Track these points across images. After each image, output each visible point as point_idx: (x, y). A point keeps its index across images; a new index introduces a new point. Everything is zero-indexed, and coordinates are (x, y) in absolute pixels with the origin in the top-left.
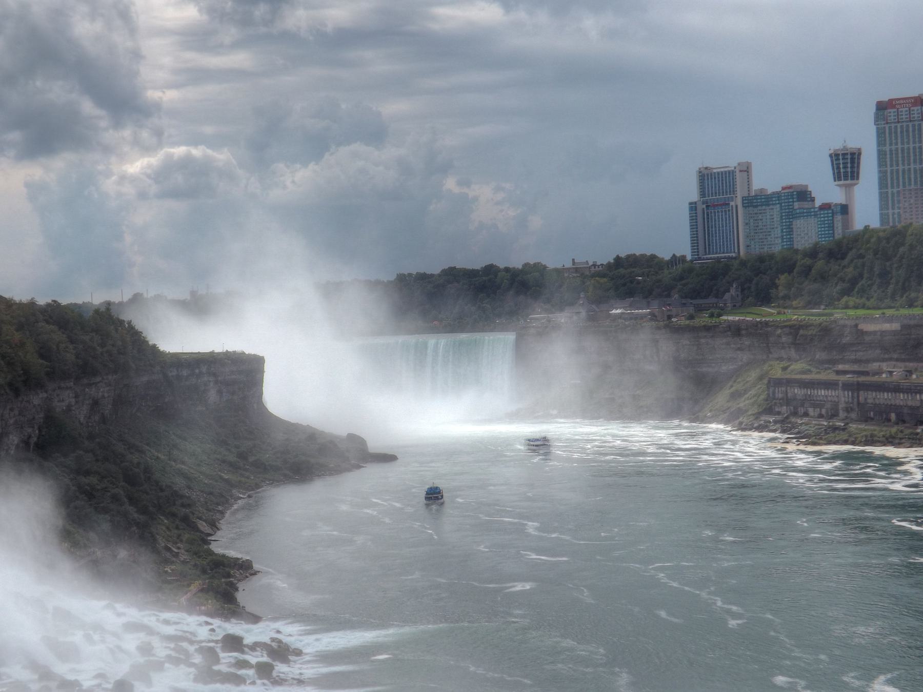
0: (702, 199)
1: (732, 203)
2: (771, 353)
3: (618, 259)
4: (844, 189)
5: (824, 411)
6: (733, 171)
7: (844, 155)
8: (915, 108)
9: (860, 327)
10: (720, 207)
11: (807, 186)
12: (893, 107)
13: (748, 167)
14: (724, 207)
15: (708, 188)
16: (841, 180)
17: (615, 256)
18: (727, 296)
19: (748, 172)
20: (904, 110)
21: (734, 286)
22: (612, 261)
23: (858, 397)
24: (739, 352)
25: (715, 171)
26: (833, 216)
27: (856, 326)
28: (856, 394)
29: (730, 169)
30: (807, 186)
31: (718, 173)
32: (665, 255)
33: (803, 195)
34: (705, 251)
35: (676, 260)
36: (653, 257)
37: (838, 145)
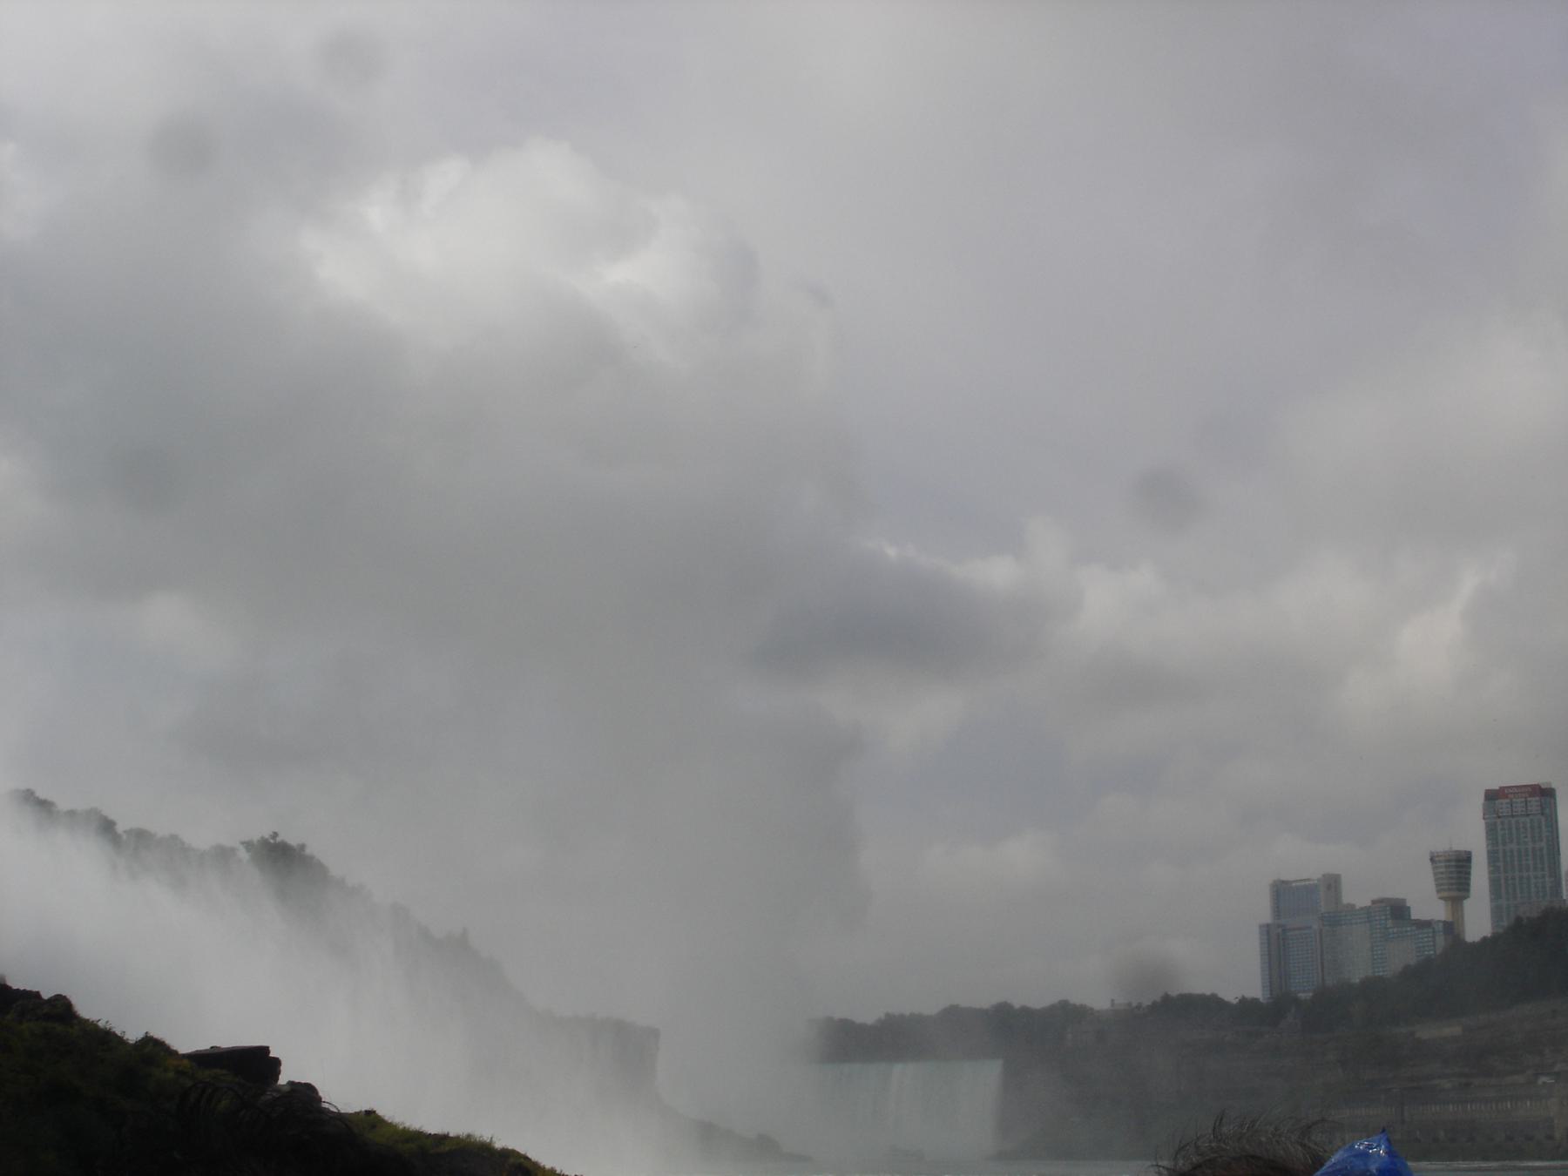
8: (1534, 799)
12: (1506, 796)
25: (1294, 884)
26: (1434, 937)
29: (1311, 882)
33: (1398, 910)
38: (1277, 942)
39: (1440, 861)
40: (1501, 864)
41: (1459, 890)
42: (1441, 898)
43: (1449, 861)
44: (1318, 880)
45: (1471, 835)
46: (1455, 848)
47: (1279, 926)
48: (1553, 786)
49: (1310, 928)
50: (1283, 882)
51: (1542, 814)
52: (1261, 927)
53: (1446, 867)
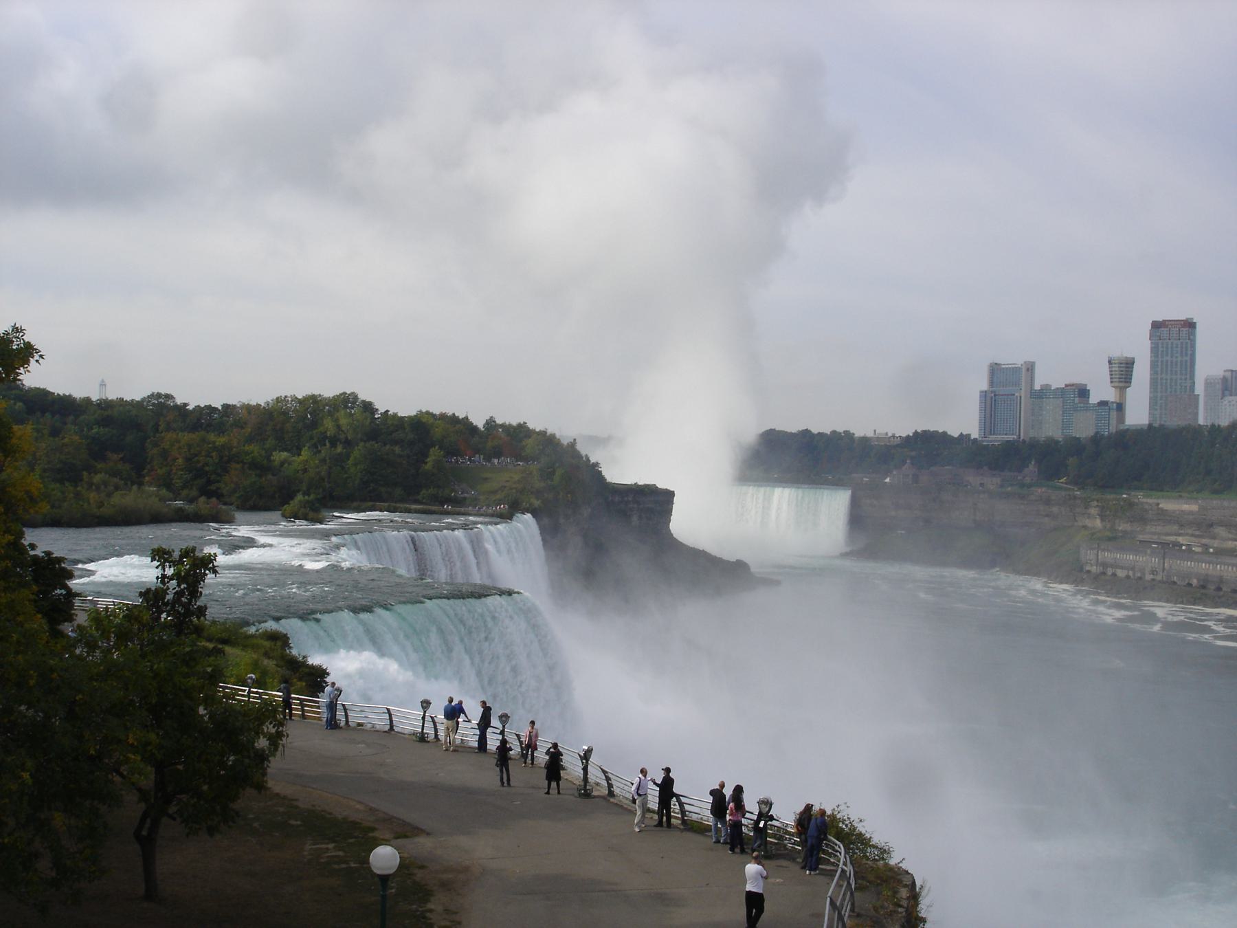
2: (1077, 521)
3: (916, 433)
4: (1118, 390)
5: (1131, 573)
6: (1019, 368)
9: (1161, 506)
11: (1086, 385)
13: (1032, 366)
17: (914, 431)
18: (1026, 471)
21: (1033, 463)
22: (911, 435)
23: (1164, 563)
24: (1046, 519)
25: (1003, 366)
27: (1158, 504)
28: (1162, 561)
30: (1086, 385)
33: (1083, 392)
35: (963, 438)
36: (945, 433)
38: (992, 403)
39: (1115, 363)
40: (1159, 369)
41: (1126, 382)
42: (1113, 387)
43: (1122, 364)
44: (1022, 365)
45: (1140, 350)
46: (1125, 355)
47: (992, 392)
48: (1194, 321)
49: (1014, 395)
50: (996, 364)
51: (1189, 339)
52: (981, 392)
53: (1119, 367)
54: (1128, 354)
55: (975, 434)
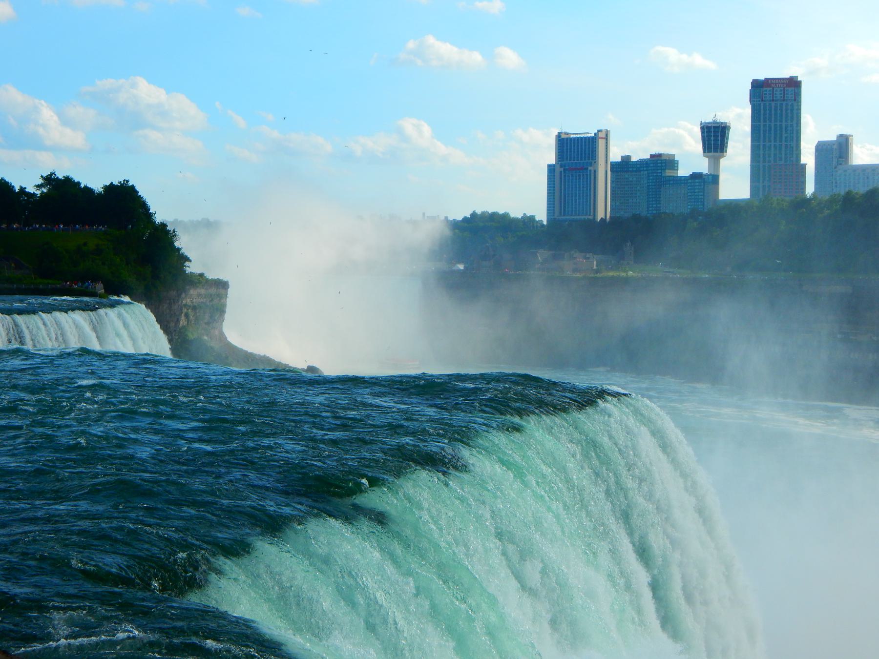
0: (560, 162)
1: (590, 168)
6: (593, 137)
7: (714, 127)
10: (578, 171)
14: (581, 171)
15: (567, 152)
16: (711, 152)
19: (607, 139)
20: (779, 89)
25: (571, 136)
29: (589, 135)
31: (574, 139)
32: (516, 213)
34: (560, 213)
37: (709, 119)
48: (799, 79)
52: (549, 166)
54: (722, 118)
55: (541, 215)
